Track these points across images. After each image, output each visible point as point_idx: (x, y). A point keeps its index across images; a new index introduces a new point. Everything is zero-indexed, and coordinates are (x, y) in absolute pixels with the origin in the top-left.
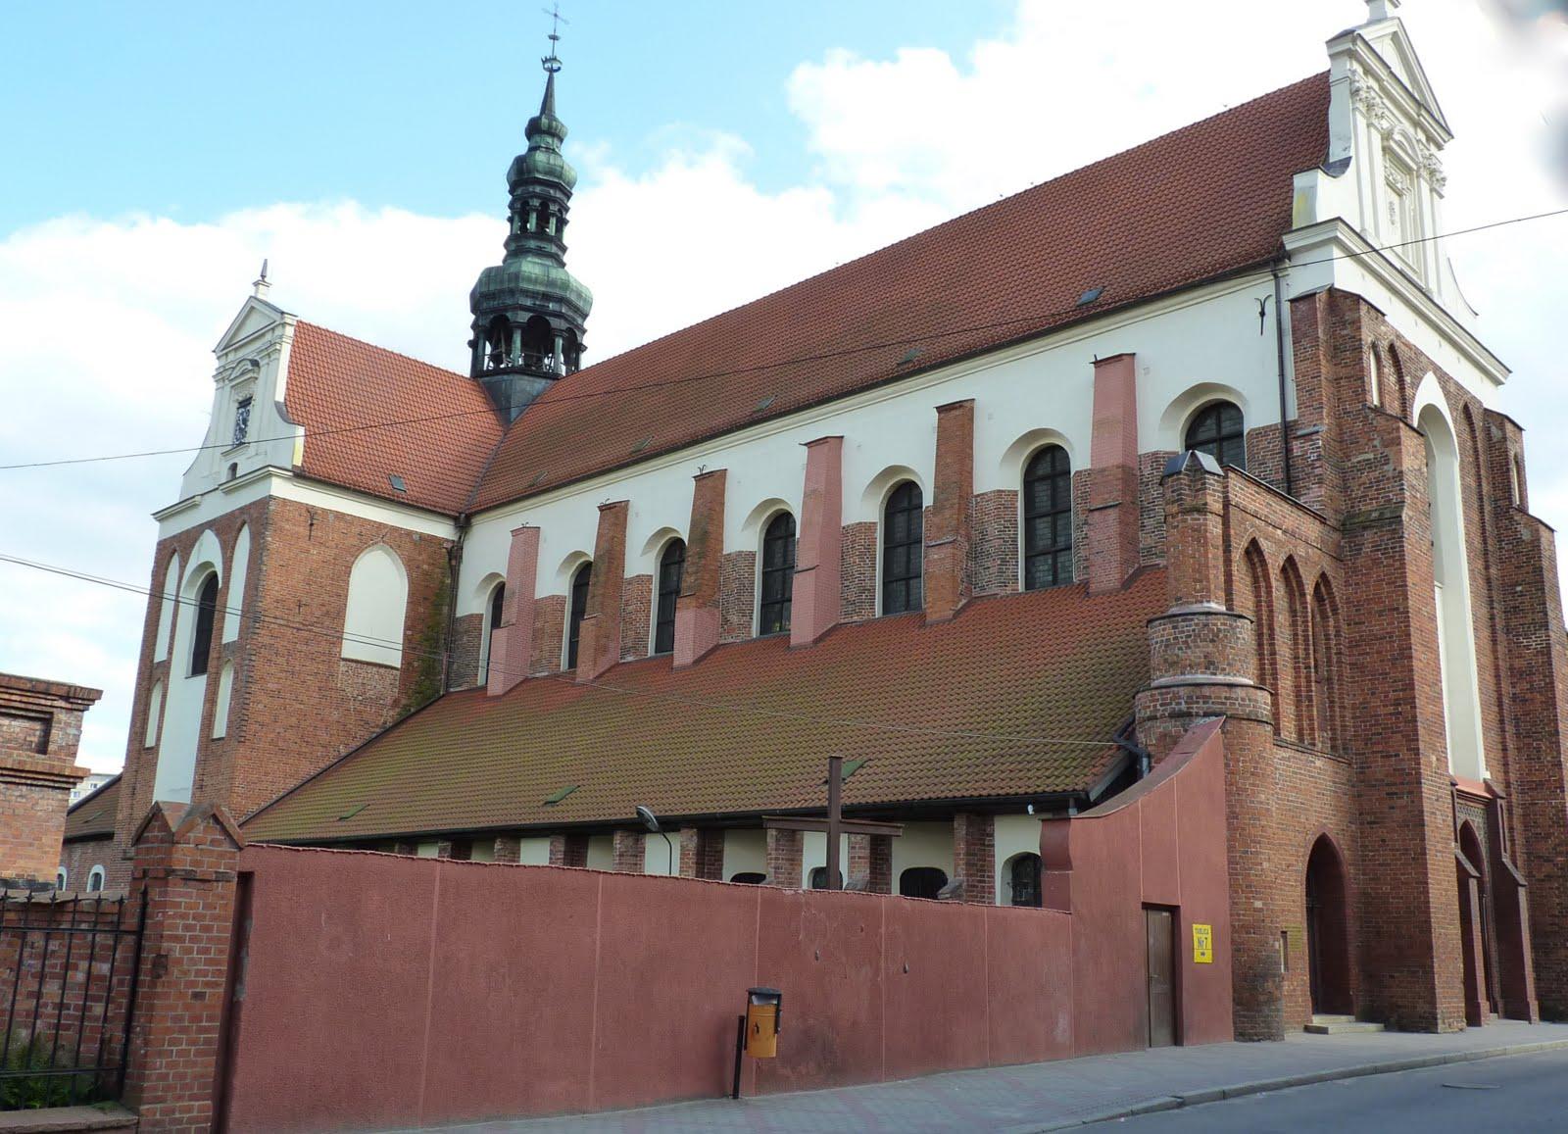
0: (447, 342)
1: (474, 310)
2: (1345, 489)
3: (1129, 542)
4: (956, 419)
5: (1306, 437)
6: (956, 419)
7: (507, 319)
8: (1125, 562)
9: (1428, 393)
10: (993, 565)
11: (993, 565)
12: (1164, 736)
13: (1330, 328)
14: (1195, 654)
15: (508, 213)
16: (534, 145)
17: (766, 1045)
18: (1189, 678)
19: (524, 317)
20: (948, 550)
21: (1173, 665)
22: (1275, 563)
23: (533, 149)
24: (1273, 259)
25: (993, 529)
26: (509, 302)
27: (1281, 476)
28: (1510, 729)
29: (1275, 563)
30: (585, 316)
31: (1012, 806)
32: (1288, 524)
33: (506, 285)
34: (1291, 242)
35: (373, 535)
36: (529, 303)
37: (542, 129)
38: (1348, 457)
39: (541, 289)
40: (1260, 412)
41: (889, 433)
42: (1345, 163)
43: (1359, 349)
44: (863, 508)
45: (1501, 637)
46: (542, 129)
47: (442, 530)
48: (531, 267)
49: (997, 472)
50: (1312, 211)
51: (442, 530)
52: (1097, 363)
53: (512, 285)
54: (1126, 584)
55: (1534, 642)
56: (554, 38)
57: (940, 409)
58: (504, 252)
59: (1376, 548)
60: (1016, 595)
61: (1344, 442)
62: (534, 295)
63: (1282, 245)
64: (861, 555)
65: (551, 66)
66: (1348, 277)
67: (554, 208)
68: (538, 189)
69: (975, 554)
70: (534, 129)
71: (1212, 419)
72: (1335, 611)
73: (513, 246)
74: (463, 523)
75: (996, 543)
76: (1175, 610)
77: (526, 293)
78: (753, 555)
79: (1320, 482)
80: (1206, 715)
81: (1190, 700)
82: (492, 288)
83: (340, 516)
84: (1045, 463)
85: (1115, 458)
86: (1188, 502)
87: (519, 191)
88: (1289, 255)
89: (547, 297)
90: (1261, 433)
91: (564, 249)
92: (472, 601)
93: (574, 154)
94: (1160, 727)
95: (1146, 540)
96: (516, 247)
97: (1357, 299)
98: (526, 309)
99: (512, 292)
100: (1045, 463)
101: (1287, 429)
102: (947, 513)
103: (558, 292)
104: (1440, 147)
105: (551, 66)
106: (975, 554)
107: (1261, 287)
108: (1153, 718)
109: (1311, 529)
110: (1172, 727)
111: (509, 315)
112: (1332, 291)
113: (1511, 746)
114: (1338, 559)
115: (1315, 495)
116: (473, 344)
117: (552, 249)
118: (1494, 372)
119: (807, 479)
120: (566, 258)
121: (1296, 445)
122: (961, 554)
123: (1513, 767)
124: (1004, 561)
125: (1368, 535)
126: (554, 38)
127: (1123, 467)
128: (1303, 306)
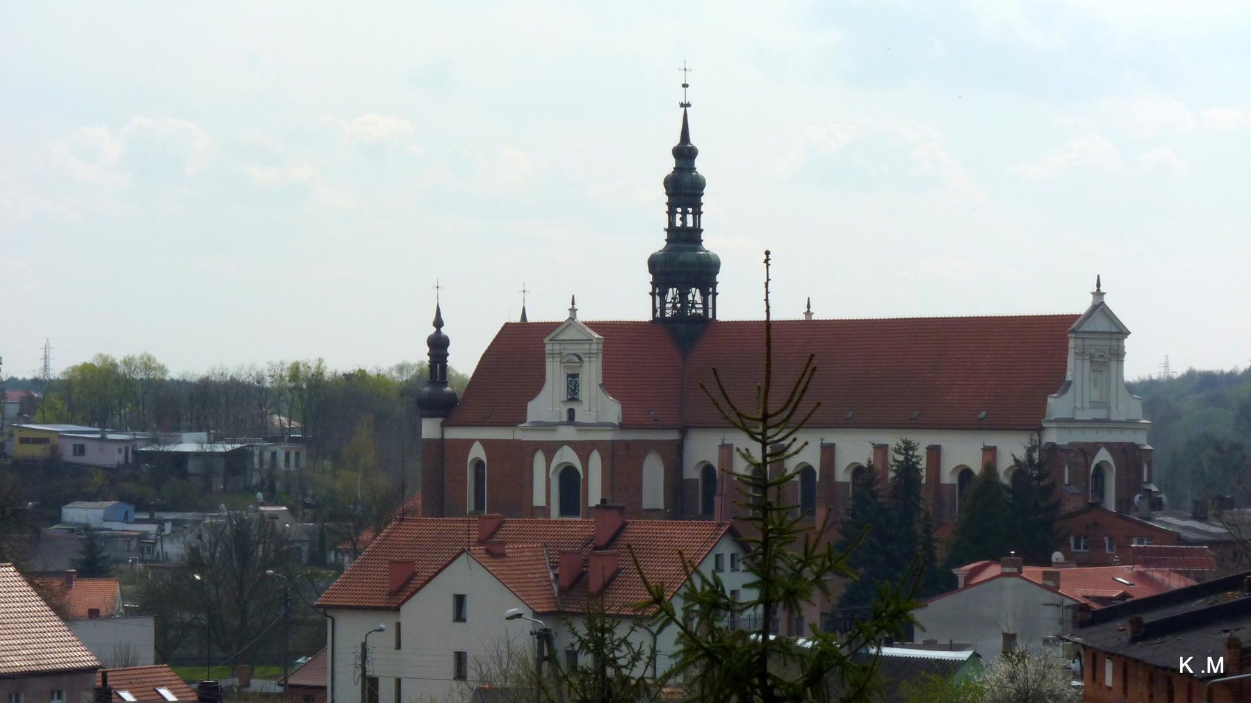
15: (666, 208)
35: (644, 448)
37: (685, 153)
42: (1070, 383)
46: (685, 153)
47: (673, 436)
51: (673, 436)
56: (685, 86)
58: (665, 235)
74: (684, 431)
83: (636, 442)
88: (1044, 428)
92: (692, 472)
93: (701, 166)
105: (685, 105)
126: (685, 86)
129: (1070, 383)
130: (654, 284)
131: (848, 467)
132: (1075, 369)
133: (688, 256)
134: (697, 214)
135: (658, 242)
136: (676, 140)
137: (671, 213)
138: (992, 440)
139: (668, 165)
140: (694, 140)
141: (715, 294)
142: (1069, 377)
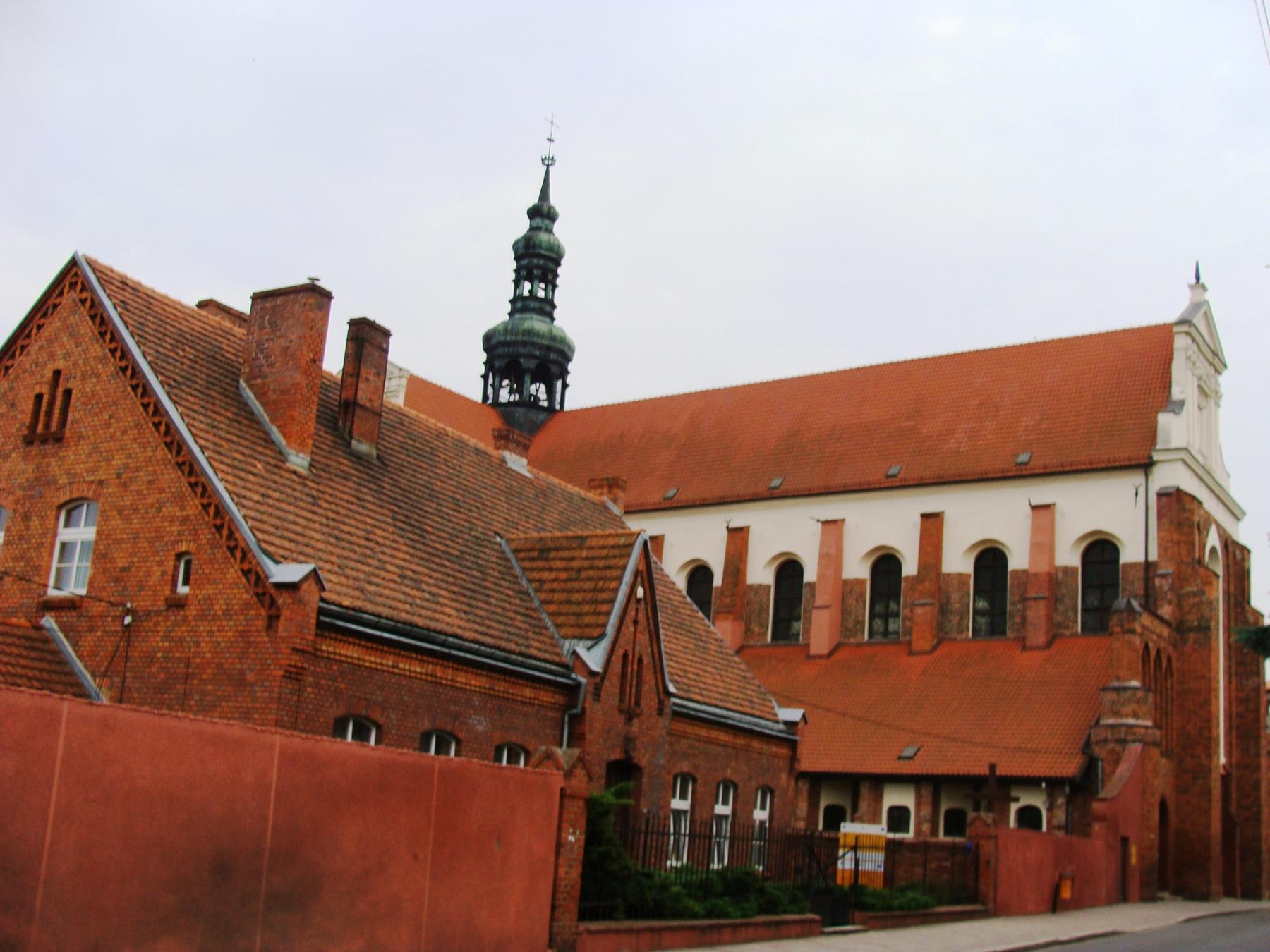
0: (465, 375)
1: (485, 350)
2: (1179, 605)
3: (1049, 619)
4: (932, 524)
5: (1164, 576)
6: (932, 524)
7: (520, 364)
8: (1047, 632)
9: (1213, 540)
10: (955, 620)
11: (955, 620)
12: (1112, 751)
13: (1177, 511)
14: (1127, 709)
15: (513, 276)
16: (535, 225)
17: (1066, 894)
18: (1124, 721)
19: (531, 364)
20: (928, 608)
21: (1116, 714)
22: (1153, 653)
23: (532, 229)
24: (1146, 466)
25: (955, 597)
26: (522, 350)
27: (1142, 592)
28: (1234, 733)
29: (1153, 653)
30: (569, 359)
31: (1030, 782)
32: (1158, 631)
33: (520, 338)
34: (1156, 457)
36: (537, 353)
37: (542, 213)
38: (1182, 587)
39: (545, 342)
40: (1131, 553)
41: (882, 524)
42: (1181, 403)
43: (1192, 526)
44: (857, 569)
45: (1234, 680)
46: (542, 213)
48: (537, 323)
49: (958, 561)
50: (1168, 440)
52: (1035, 508)
53: (526, 338)
54: (1049, 645)
55: (1251, 683)
56: (550, 140)
57: (925, 516)
58: (508, 308)
59: (1195, 642)
60: (967, 639)
61: (1180, 579)
62: (541, 347)
63: (1151, 457)
64: (857, 600)
65: (548, 162)
66: (1190, 485)
67: (550, 277)
68: (541, 262)
69: (943, 611)
70: (534, 213)
71: (1100, 550)
72: (1172, 674)
73: (519, 305)
75: (957, 606)
76: (1116, 684)
77: (533, 345)
78: (769, 587)
79: (1170, 602)
80: (1135, 741)
81: (1126, 733)
82: (509, 338)
84: (990, 559)
85: (1043, 568)
86: (1126, 627)
87: (525, 262)
89: (549, 349)
90: (1133, 566)
91: (554, 307)
93: (562, 232)
94: (1110, 746)
95: (1059, 618)
96: (520, 305)
97: (1193, 498)
98: (534, 357)
99: (524, 344)
100: (990, 559)
101: (1148, 566)
102: (927, 584)
103: (558, 346)
104: (1218, 372)
105: (548, 162)
106: (943, 611)
107: (1137, 479)
108: (1105, 741)
109: (1165, 632)
110: (1118, 748)
111: (522, 360)
112: (1178, 490)
113: (1234, 742)
114: (1174, 646)
115: (1166, 610)
116: (485, 377)
117: (546, 308)
118: (1236, 514)
119: (822, 544)
120: (556, 314)
121: (1157, 582)
122: (936, 611)
123: (1235, 755)
124: (962, 618)
125: (1192, 636)
126: (550, 140)
127: (1049, 574)
128: (1164, 499)
129: (1181, 403)
130: (489, 365)
131: (775, 558)
132: (1183, 383)
133: (537, 323)
134: (552, 285)
135: (497, 313)
136: (534, 199)
137: (517, 283)
138: (1042, 492)
139: (522, 226)
140: (555, 200)
141: (565, 386)
142: (1176, 393)
